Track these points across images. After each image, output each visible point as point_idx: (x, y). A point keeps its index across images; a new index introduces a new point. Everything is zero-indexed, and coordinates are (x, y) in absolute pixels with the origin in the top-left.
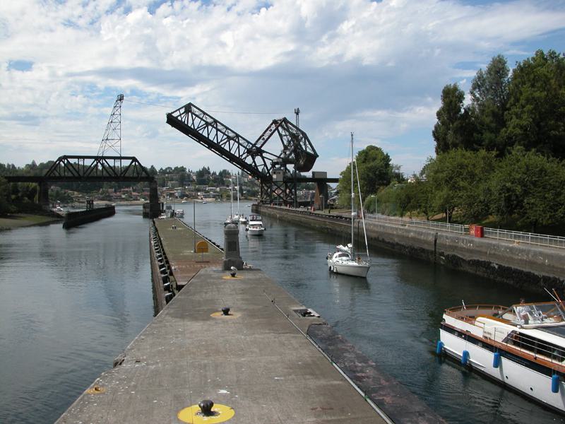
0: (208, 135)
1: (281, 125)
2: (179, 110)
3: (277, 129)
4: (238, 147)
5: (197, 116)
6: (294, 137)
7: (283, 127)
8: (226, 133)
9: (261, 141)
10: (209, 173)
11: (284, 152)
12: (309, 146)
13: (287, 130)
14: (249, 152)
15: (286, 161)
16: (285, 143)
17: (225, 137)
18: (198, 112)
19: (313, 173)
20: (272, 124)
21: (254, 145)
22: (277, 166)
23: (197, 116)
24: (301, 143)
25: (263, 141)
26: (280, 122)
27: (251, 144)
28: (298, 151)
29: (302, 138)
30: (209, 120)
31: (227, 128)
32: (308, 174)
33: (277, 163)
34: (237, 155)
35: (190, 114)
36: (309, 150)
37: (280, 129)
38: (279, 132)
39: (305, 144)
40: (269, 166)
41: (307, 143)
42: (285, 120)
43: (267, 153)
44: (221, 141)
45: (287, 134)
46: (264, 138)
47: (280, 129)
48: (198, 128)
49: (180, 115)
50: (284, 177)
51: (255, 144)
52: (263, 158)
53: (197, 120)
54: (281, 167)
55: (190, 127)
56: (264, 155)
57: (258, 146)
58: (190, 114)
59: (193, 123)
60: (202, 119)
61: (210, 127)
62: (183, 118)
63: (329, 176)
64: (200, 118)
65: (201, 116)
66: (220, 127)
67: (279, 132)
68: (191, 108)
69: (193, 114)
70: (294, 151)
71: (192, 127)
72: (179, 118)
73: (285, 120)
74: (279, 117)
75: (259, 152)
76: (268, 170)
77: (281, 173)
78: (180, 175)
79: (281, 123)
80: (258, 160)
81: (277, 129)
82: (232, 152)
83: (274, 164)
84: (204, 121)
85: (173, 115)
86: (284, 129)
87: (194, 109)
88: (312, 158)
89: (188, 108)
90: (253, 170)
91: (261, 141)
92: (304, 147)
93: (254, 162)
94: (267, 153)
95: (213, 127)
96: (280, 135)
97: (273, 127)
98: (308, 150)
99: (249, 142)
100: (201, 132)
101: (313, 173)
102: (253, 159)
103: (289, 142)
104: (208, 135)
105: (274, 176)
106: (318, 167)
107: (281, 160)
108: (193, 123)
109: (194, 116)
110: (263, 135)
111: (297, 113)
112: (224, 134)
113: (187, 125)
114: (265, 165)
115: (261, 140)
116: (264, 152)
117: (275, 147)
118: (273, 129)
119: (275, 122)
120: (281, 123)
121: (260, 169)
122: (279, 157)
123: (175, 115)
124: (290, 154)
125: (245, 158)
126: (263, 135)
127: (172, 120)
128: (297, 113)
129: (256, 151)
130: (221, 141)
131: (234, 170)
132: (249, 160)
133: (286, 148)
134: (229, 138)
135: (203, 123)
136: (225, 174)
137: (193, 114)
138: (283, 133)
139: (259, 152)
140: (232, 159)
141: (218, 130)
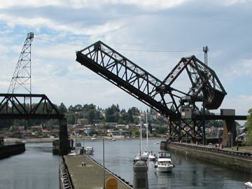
0: (118, 72)
1: (189, 63)
2: (88, 48)
3: (186, 67)
4: (148, 85)
5: (106, 54)
6: (201, 73)
7: (191, 65)
8: (135, 71)
9: (170, 79)
10: (118, 110)
11: (193, 89)
12: (217, 83)
13: (196, 67)
14: (158, 90)
15: (194, 99)
16: (194, 80)
17: (134, 75)
18: (107, 51)
19: (222, 110)
20: (180, 62)
21: (163, 83)
22: (186, 104)
23: (106, 54)
24: (210, 81)
26: (188, 60)
27: (160, 81)
28: (206, 89)
29: (210, 76)
30: (119, 58)
31: (136, 66)
32: (217, 112)
33: (186, 101)
34: (146, 92)
35: (99, 52)
36: (218, 88)
37: (189, 66)
38: (187, 70)
39: (213, 82)
40: (178, 104)
41: (216, 81)
42: (193, 58)
43: (176, 90)
44: (131, 79)
45: (196, 71)
46: (173, 76)
48: (107, 65)
49: (90, 53)
50: (193, 115)
51: (164, 82)
52: (172, 95)
53: (107, 58)
54: (189, 105)
55: (100, 65)
56: (173, 92)
57: (167, 83)
58: (99, 52)
59: (102, 61)
60: (111, 57)
61: (119, 65)
62: (93, 56)
63: (237, 114)
64: (109, 56)
65: (111, 54)
66: (129, 65)
67: (187, 70)
68: (100, 46)
69: (102, 52)
70: (203, 89)
71: (102, 65)
72: (89, 56)
73: (193, 58)
74: (188, 55)
75: (168, 90)
76: (177, 108)
77: (190, 110)
78: (90, 113)
79: (190, 61)
80: (167, 97)
81: (186, 67)
82: (141, 90)
83: (182, 102)
84: (113, 58)
85: (82, 53)
86: (193, 67)
87: (103, 47)
88: (220, 96)
89: (98, 46)
90: (161, 107)
91: (170, 79)
92: (212, 85)
93: (163, 99)
94: (176, 90)
95: (122, 64)
96: (189, 73)
97: (182, 65)
98: (217, 88)
99: (157, 80)
100: (110, 70)
101: (222, 110)
102: (162, 96)
103: (198, 80)
104: (118, 72)
105: (183, 114)
106: (226, 104)
107: (189, 98)
108: (102, 61)
109: (103, 55)
110: (172, 73)
111: (206, 52)
112: (133, 72)
113: (97, 63)
114: (174, 102)
115: (170, 78)
116: (173, 89)
117: (183, 85)
118: (182, 67)
119: (183, 60)
120: (190, 61)
121: (169, 106)
122: (188, 95)
123: (84, 53)
124: (199, 92)
125: (154, 95)
126: (172, 73)
127: (81, 58)
128: (206, 52)
129: (165, 89)
130: (131, 79)
131: (143, 107)
132: (158, 98)
133: (194, 85)
134: (138, 76)
135: (112, 61)
136: (134, 111)
137: (102, 52)
138: (192, 71)
139: (168, 90)
140: (142, 96)
141: (127, 68)
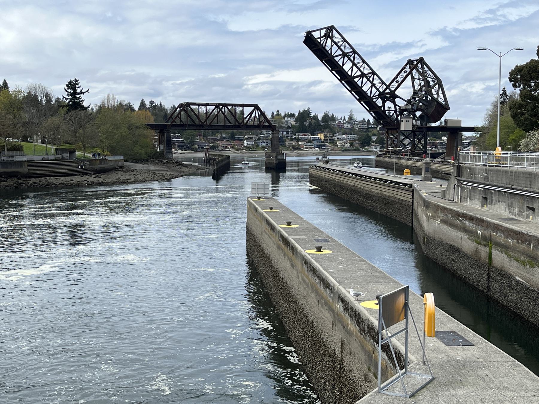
1: (416, 67)
3: (411, 73)
7: (418, 71)
9: (395, 84)
13: (423, 74)
20: (406, 65)
24: (434, 92)
25: (397, 84)
27: (386, 85)
29: (435, 85)
37: (414, 71)
41: (440, 92)
47: (414, 71)
64: (357, 67)
71: (349, 73)
76: (397, 116)
79: (417, 64)
81: (411, 73)
88: (444, 108)
91: (395, 84)
96: (413, 79)
119: (410, 62)
120: (417, 64)
126: (396, 77)
132: (379, 102)
